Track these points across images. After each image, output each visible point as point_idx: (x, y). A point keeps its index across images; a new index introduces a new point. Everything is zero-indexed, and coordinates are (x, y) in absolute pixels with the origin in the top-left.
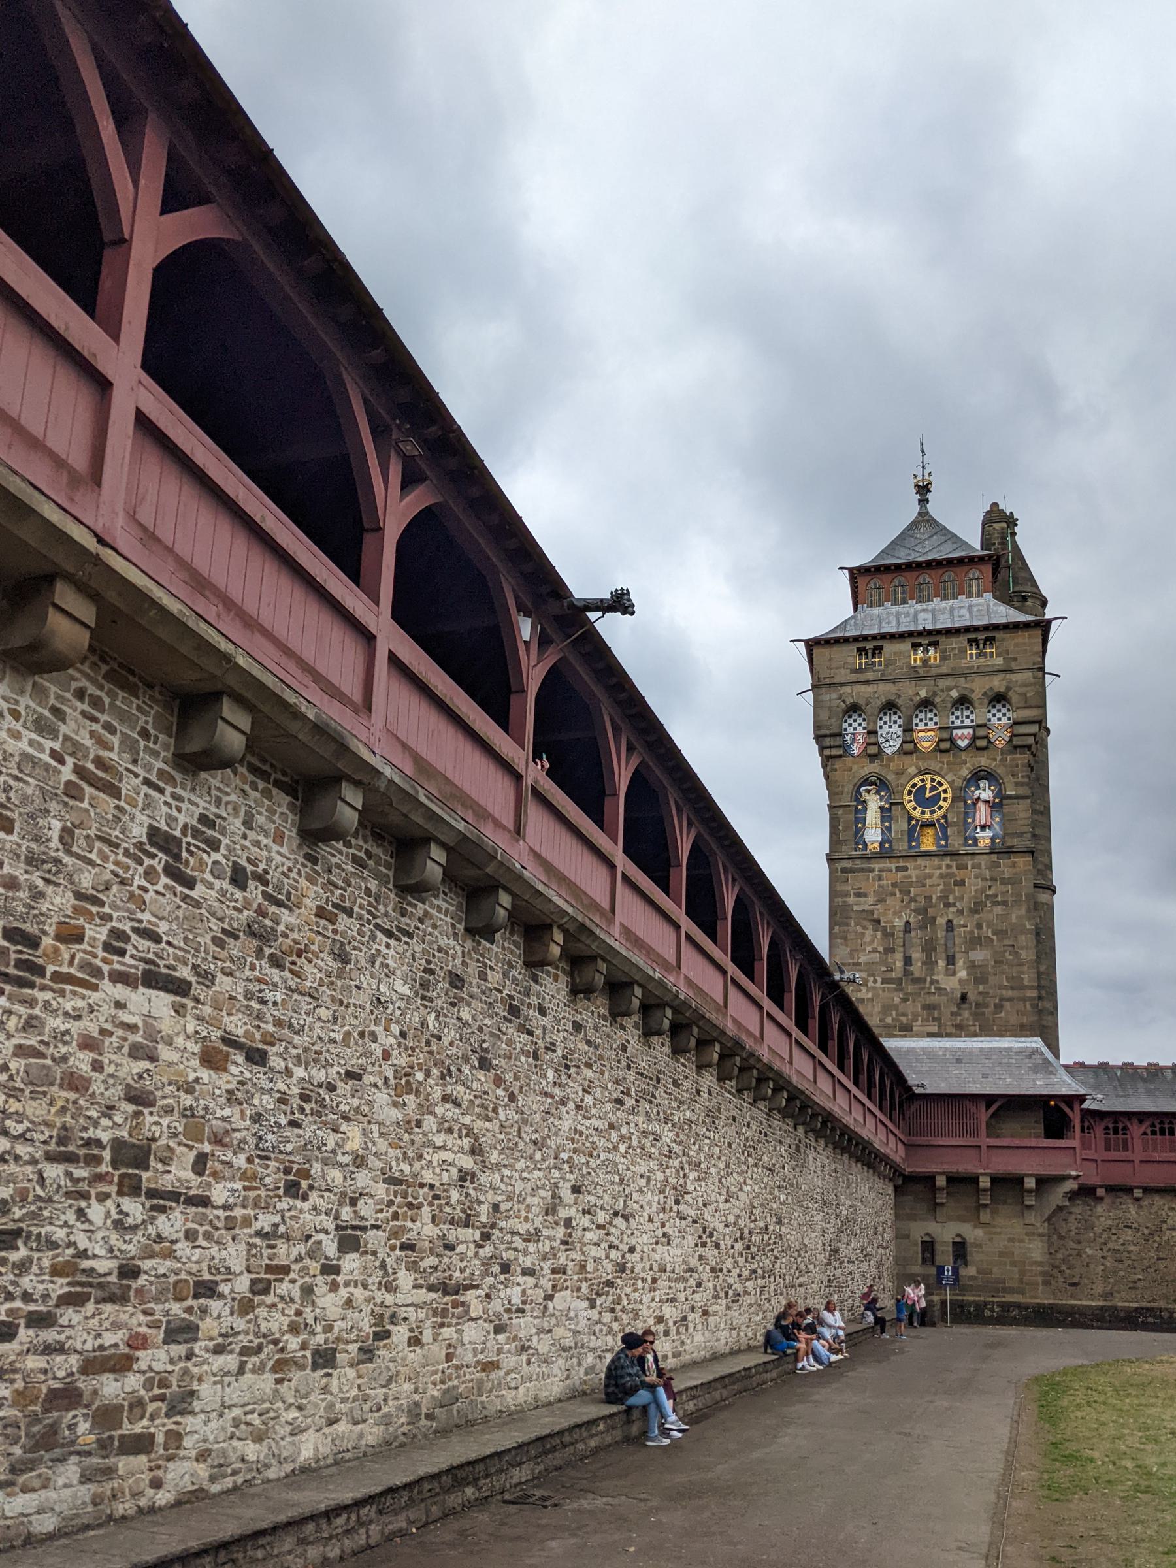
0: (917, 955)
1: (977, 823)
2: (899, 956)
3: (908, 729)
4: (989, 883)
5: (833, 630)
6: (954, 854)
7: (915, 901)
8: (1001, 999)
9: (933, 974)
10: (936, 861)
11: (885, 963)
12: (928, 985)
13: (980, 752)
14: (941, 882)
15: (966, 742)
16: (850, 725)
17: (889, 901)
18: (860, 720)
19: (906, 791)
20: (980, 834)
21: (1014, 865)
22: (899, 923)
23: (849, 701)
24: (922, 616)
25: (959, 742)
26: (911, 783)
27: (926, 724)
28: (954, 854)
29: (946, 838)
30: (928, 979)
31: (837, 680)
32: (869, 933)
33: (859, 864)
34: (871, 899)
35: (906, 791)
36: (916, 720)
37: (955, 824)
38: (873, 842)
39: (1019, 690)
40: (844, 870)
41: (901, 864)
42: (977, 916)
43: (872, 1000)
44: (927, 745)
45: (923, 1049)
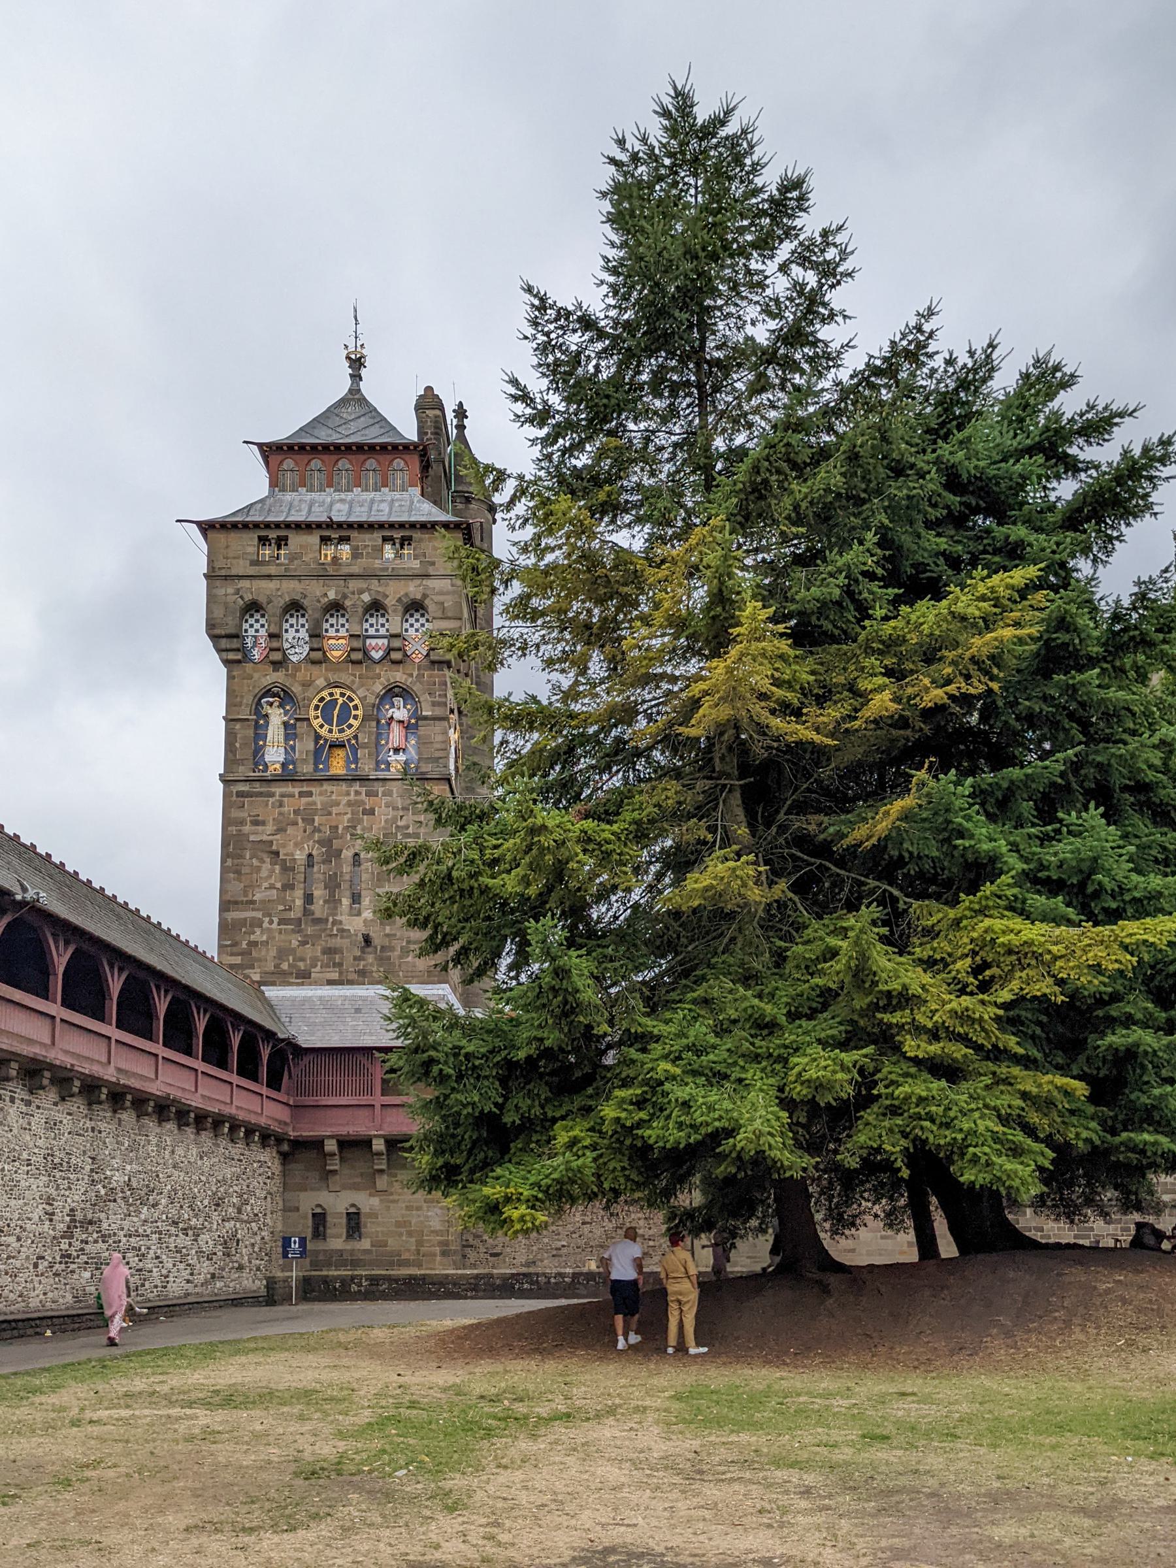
0: (319, 893)
1: (390, 746)
2: (299, 893)
5: (234, 514)
6: (364, 780)
7: (319, 831)
8: (409, 942)
9: (336, 914)
10: (344, 787)
11: (284, 903)
12: (329, 926)
13: (394, 667)
14: (349, 810)
15: (381, 653)
16: (252, 626)
17: (290, 830)
18: (263, 621)
19: (312, 706)
20: (393, 758)
22: (300, 856)
24: (338, 506)
26: (318, 697)
27: (337, 631)
28: (364, 780)
29: (356, 761)
31: (234, 572)
32: (267, 866)
34: (270, 828)
35: (312, 706)
36: (326, 626)
37: (365, 746)
38: (274, 763)
40: (240, 794)
41: (305, 789)
44: (335, 655)
45: (321, 998)
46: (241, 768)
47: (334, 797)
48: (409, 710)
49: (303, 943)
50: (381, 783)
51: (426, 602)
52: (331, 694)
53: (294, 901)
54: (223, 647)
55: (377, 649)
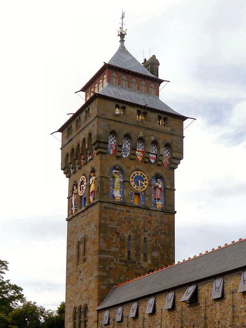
0: (133, 251)
3: (134, 149)
6: (148, 209)
7: (133, 227)
10: (141, 210)
18: (113, 138)
21: (169, 218)
22: (126, 236)
25: (151, 160)
28: (148, 209)
32: (115, 238)
33: (111, 206)
34: (116, 223)
40: (105, 208)
41: (128, 209)
43: (115, 269)
47: (138, 214)
51: (172, 145)
53: (124, 253)
54: (102, 146)
55: (152, 158)
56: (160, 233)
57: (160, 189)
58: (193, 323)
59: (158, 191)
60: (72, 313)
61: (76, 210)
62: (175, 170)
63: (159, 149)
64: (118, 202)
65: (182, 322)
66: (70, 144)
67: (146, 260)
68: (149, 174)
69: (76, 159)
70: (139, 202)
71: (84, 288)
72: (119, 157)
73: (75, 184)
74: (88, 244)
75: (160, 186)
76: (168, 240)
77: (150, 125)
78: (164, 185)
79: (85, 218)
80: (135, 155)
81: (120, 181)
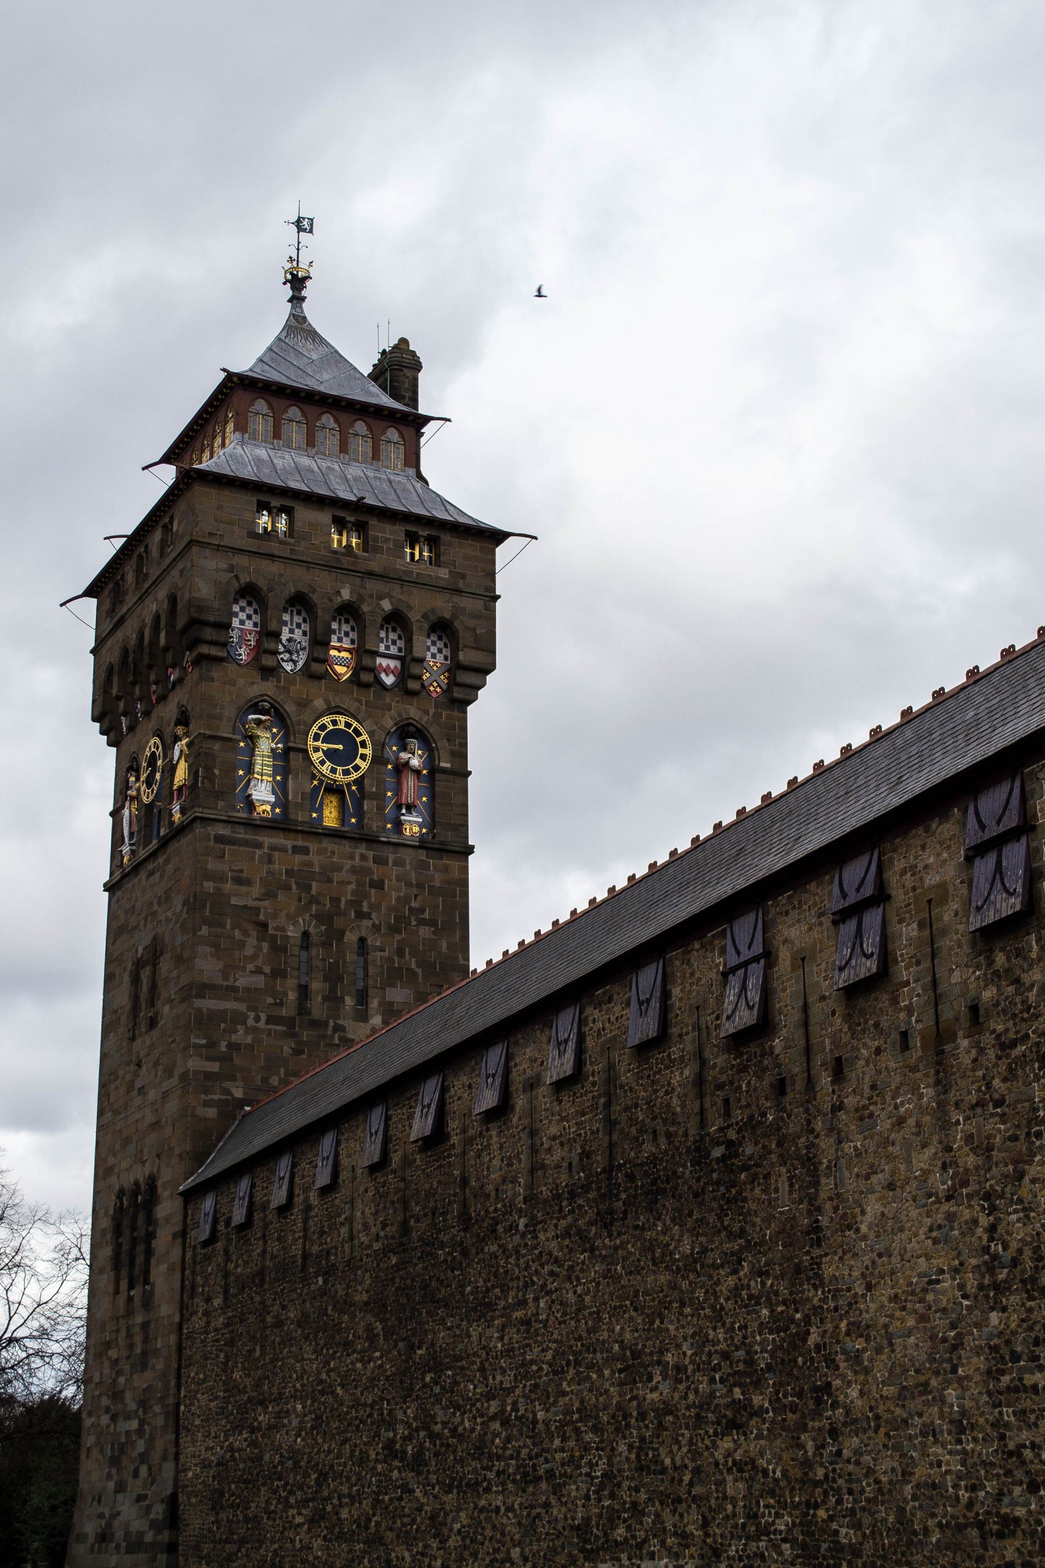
2: (291, 982)
3: (320, 642)
4: (415, 891)
6: (372, 841)
7: (318, 903)
10: (346, 847)
12: (330, 1033)
14: (353, 878)
21: (446, 869)
22: (293, 932)
23: (245, 578)
25: (383, 676)
27: (340, 640)
28: (372, 841)
29: (360, 814)
30: (331, 1023)
32: (252, 941)
33: (242, 834)
34: (256, 890)
37: (373, 797)
38: (264, 803)
39: (471, 623)
40: (220, 839)
41: (300, 843)
42: (397, 937)
46: (221, 804)
48: (421, 756)
49: (297, 1052)
50: (391, 848)
52: (334, 722)
53: (286, 995)
54: (208, 637)
55: (387, 671)
56: (414, 923)
57: (417, 772)
58: (432, 1204)
59: (410, 783)
60: (111, 1212)
61: (133, 852)
62: (471, 709)
63: (409, 641)
64: (262, 819)
65: (405, 1203)
66: (119, 635)
67: (363, 1016)
68: (376, 724)
69: (134, 683)
70: (343, 817)
71: (150, 1118)
72: (270, 672)
73: (130, 769)
74: (165, 965)
75: (415, 762)
76: (444, 945)
77: (376, 564)
78: (431, 762)
79: (157, 876)
80: (325, 660)
81: (273, 750)
